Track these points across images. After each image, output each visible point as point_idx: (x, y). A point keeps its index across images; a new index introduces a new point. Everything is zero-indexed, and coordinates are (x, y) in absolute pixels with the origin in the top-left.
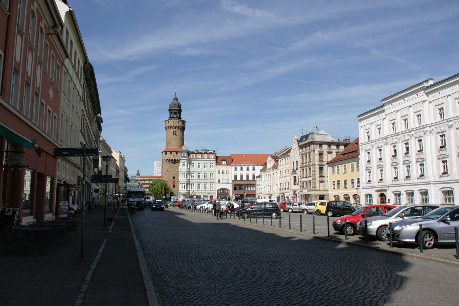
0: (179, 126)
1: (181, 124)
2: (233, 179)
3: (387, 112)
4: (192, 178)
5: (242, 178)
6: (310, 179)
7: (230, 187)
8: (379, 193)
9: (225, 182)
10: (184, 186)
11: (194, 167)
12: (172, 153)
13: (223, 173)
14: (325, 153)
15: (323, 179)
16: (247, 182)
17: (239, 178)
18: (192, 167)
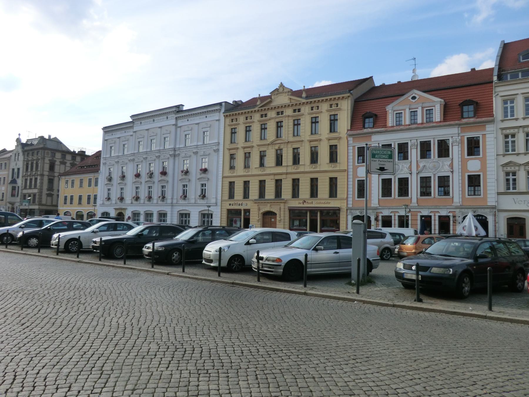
3: (135, 129)
6: (35, 191)
8: (118, 211)
14: (58, 163)
15: (51, 192)
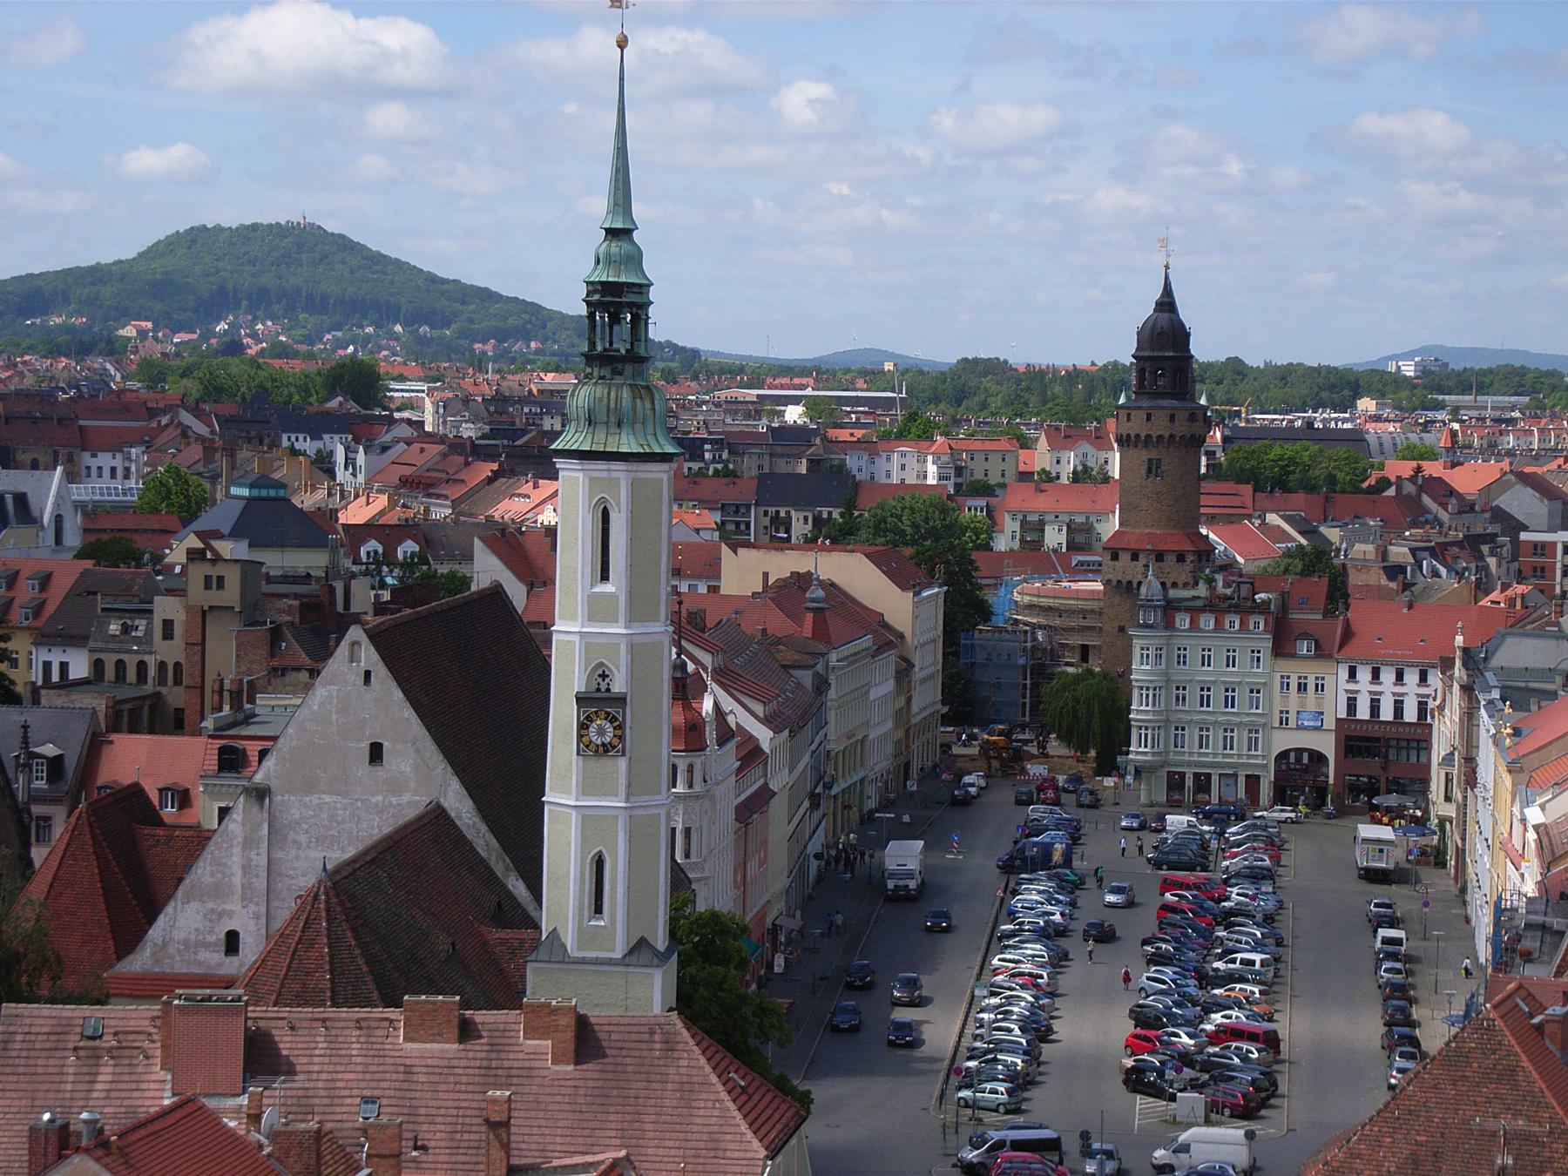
0: (1171, 436)
1: (1181, 428)
2: (1342, 714)
4: (1177, 705)
5: (1375, 707)
7: (1327, 745)
9: (1306, 723)
10: (1146, 735)
11: (1185, 663)
12: (1141, 556)
13: (1302, 688)
16: (1394, 730)
17: (1363, 713)
18: (1179, 662)
